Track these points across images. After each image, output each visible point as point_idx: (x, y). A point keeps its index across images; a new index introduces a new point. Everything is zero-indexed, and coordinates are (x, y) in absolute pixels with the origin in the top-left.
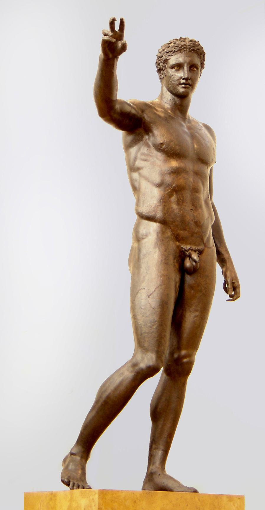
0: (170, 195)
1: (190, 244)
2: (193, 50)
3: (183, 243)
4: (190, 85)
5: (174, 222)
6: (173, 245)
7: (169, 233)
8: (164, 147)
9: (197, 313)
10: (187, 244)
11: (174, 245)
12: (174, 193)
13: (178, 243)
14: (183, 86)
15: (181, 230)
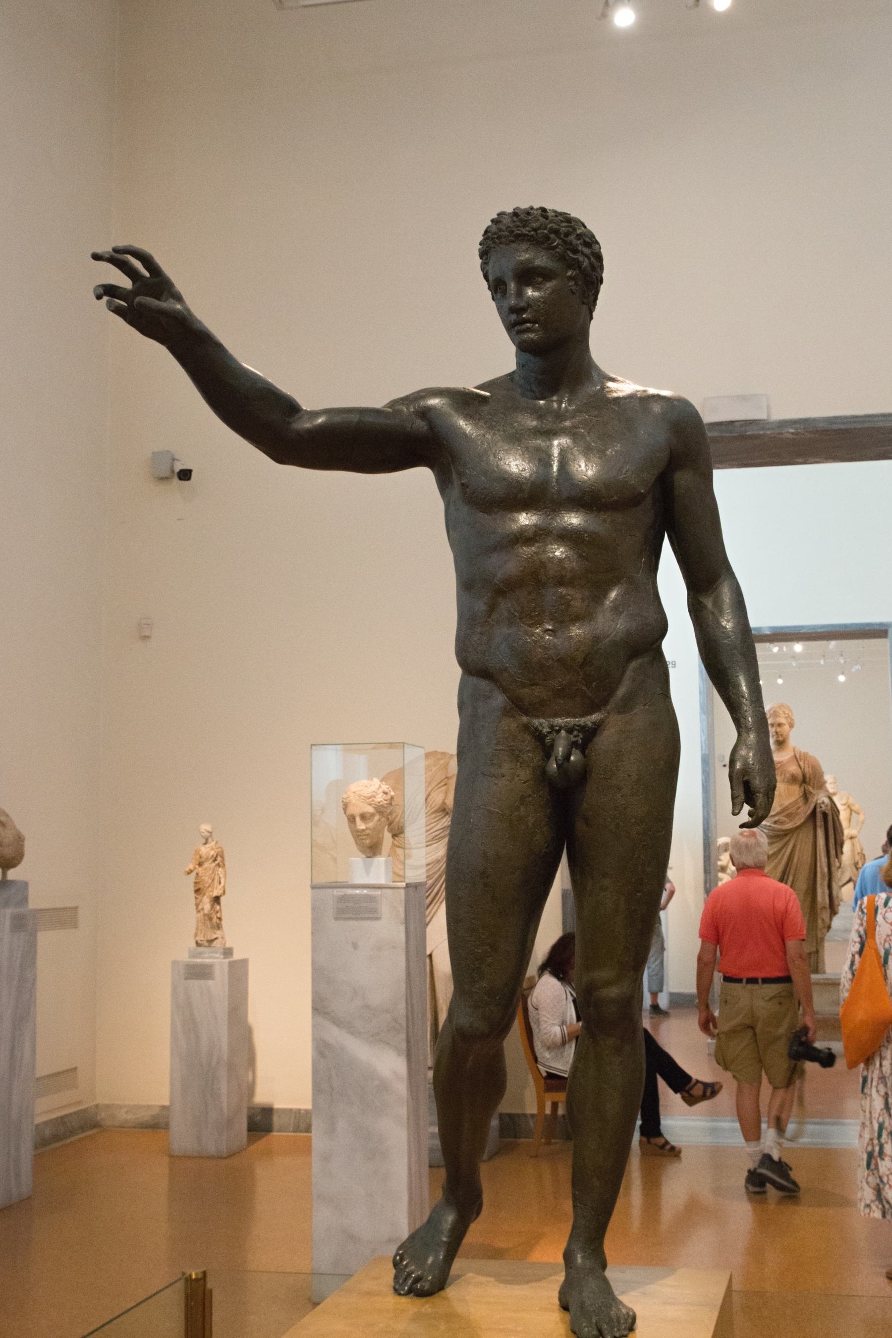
0: (492, 608)
1: (556, 715)
2: (518, 236)
3: (538, 717)
4: (534, 322)
5: (506, 669)
6: (511, 725)
7: (499, 699)
8: (468, 490)
9: (606, 882)
10: (543, 716)
11: (514, 725)
12: (500, 599)
13: (525, 719)
14: (518, 328)
15: (524, 686)
